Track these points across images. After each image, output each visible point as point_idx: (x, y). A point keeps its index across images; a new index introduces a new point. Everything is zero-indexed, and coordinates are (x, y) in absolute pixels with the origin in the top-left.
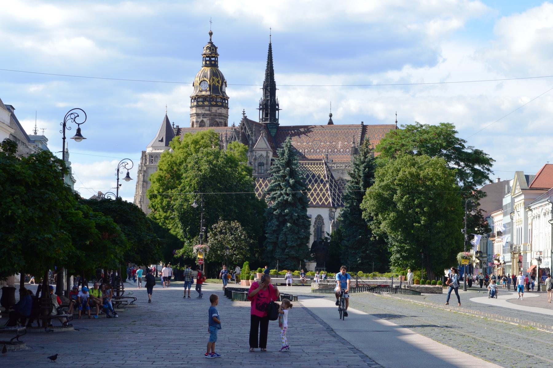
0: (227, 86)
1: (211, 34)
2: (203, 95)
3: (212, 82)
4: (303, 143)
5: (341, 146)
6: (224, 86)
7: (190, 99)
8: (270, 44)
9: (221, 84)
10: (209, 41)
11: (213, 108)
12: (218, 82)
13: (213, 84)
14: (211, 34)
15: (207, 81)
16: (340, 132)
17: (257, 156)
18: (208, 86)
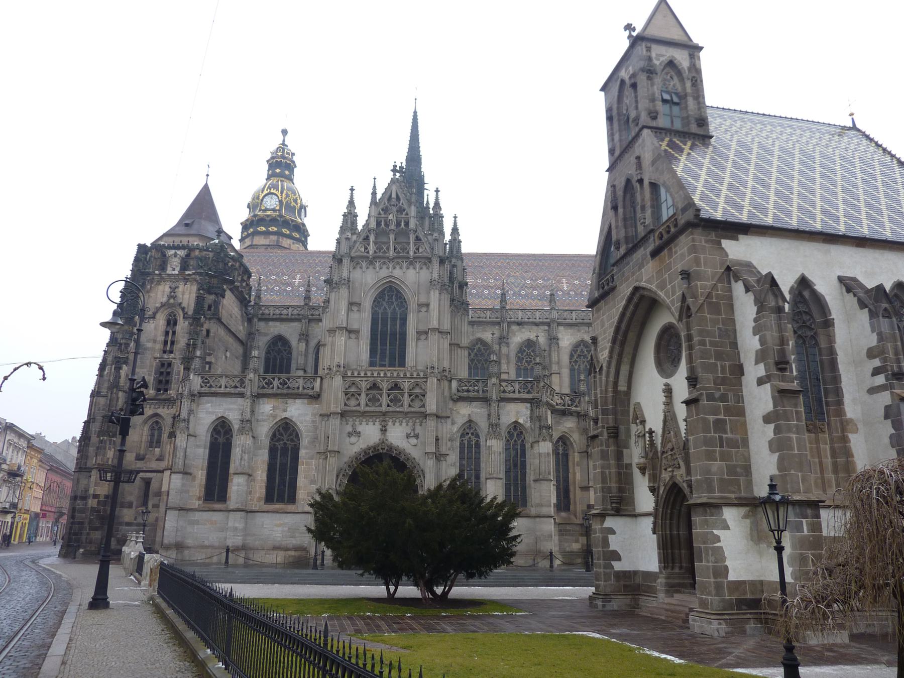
0: (307, 216)
1: (285, 132)
2: (268, 216)
3: (285, 198)
4: (488, 279)
5: (567, 287)
6: (303, 211)
7: (241, 227)
8: (415, 112)
9: (299, 205)
10: (282, 142)
11: (285, 239)
12: (295, 201)
13: (287, 202)
14: (285, 132)
15: (276, 195)
16: (558, 265)
17: (657, 63)
18: (277, 203)
